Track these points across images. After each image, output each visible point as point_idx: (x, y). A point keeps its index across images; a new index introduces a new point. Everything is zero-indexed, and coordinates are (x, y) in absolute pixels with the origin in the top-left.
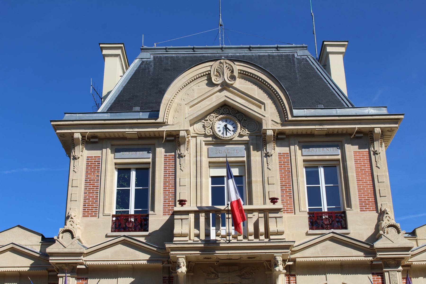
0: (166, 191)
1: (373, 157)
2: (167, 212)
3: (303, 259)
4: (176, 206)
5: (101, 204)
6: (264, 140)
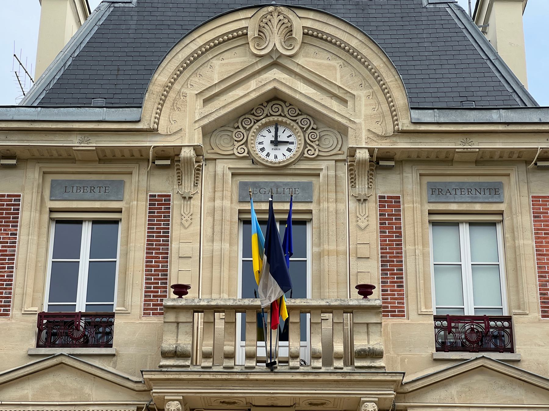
0: (152, 266)
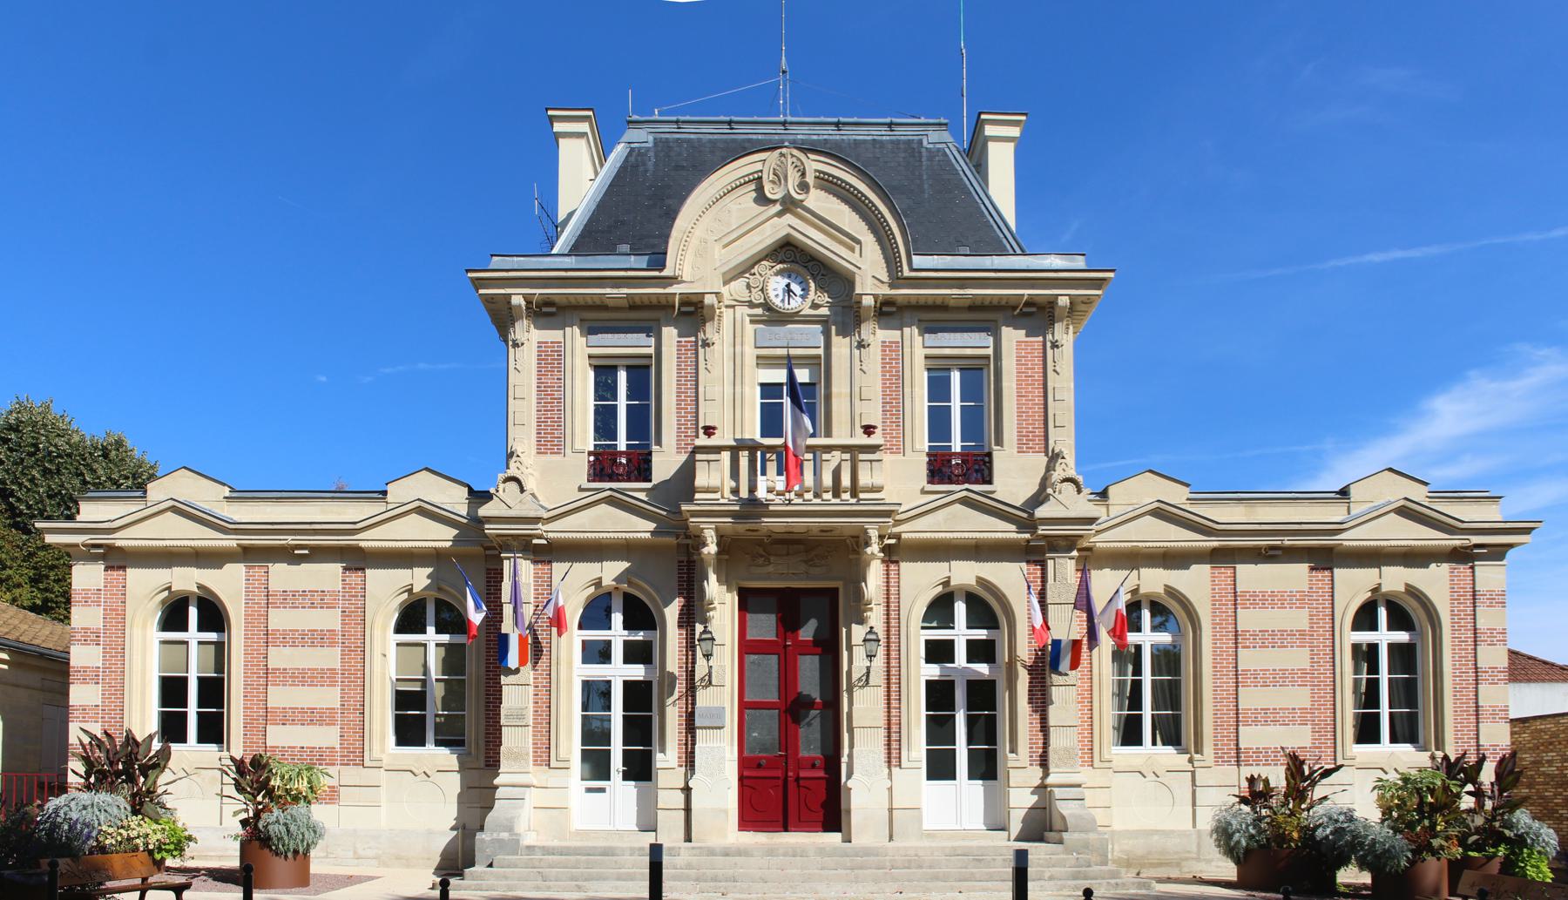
1: (1050, 352)
5: (568, 431)
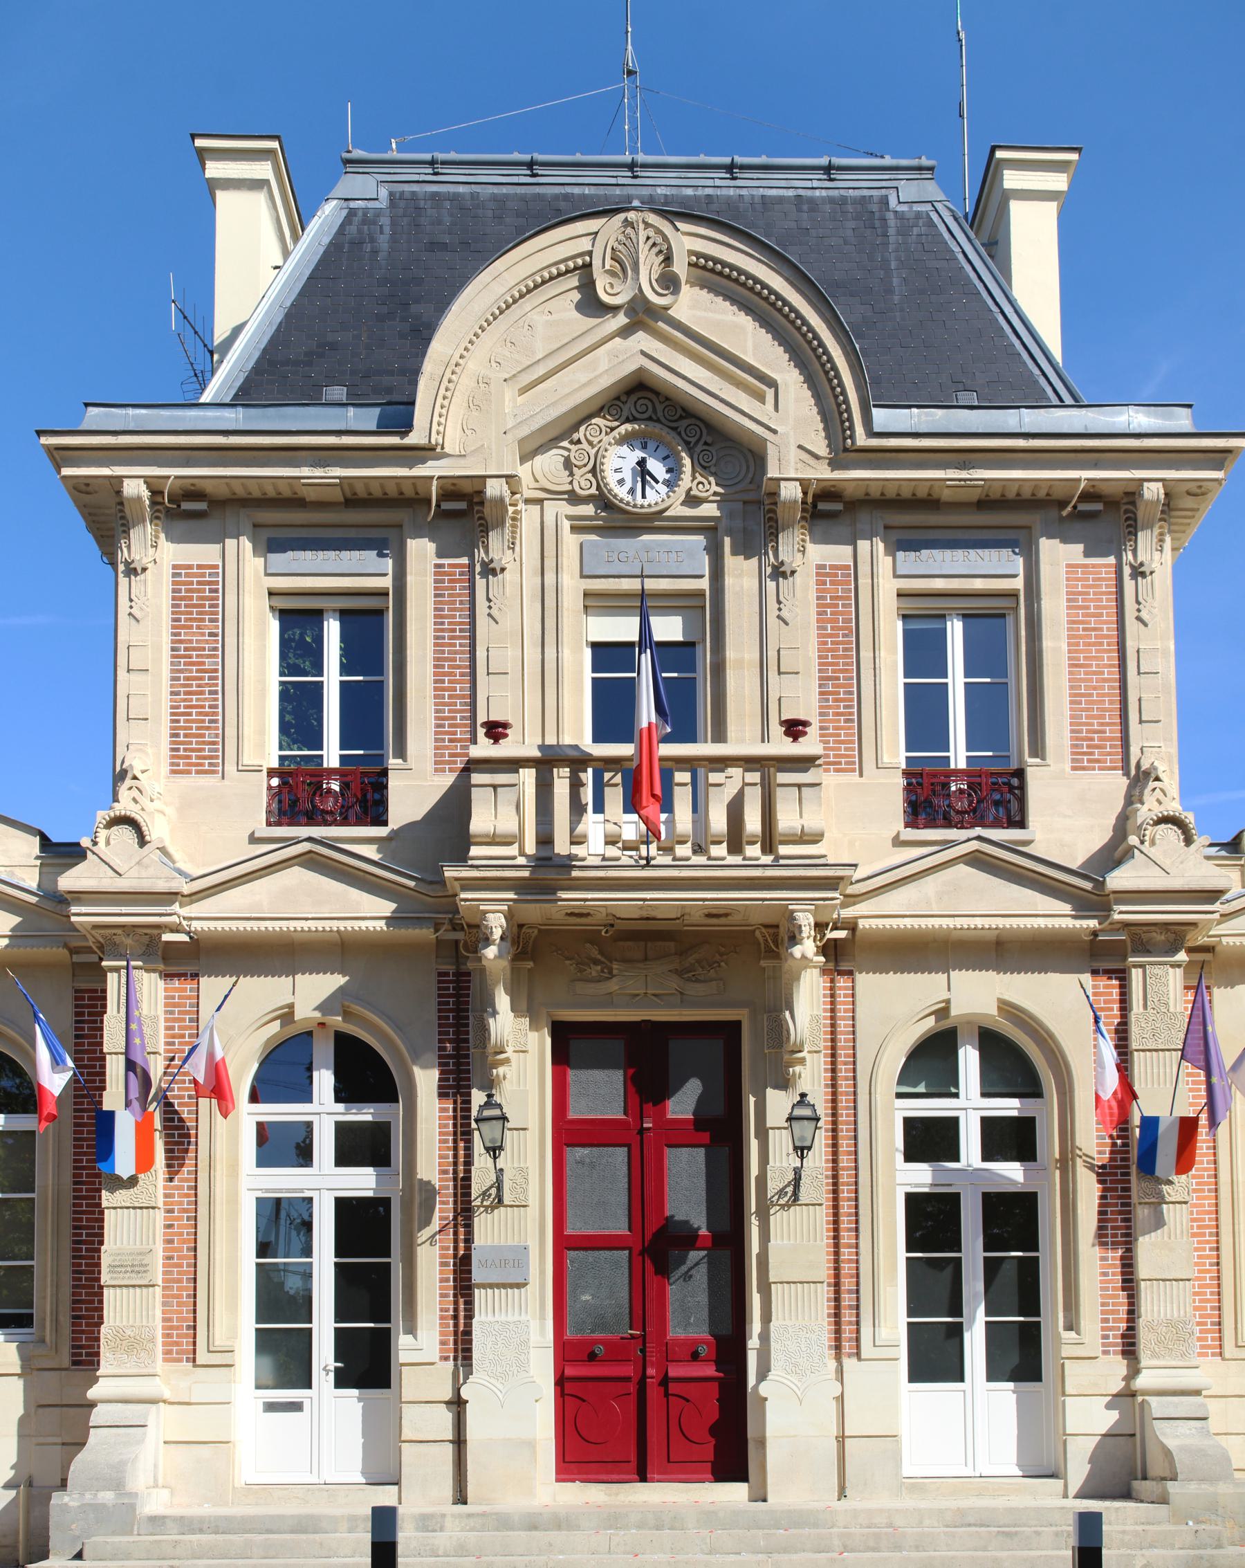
0: (444, 689)
1: (1129, 585)
2: (449, 762)
3: (880, 923)
4: (475, 743)
5: (230, 731)
6: (770, 519)
